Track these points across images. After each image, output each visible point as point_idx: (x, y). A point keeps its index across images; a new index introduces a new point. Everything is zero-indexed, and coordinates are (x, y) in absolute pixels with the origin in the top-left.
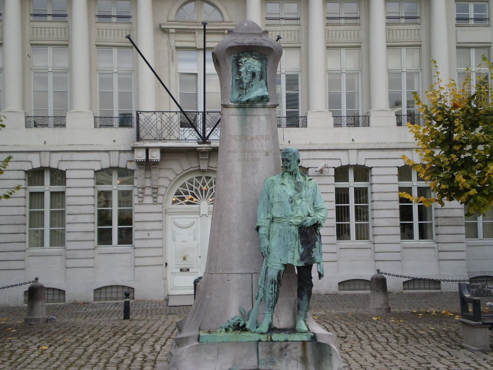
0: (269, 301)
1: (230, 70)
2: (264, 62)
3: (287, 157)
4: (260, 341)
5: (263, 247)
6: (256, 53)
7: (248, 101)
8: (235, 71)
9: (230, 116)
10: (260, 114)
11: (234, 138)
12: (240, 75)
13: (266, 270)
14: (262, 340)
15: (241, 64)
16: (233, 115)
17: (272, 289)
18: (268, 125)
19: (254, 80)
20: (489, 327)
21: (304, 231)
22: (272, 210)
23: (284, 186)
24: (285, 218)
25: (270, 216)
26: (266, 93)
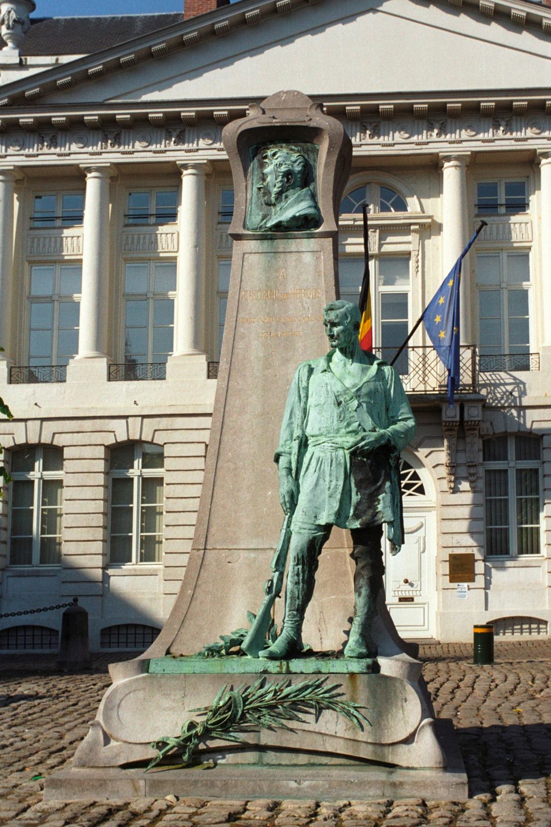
4: (265, 672)
12: (264, 180)
14: (269, 670)
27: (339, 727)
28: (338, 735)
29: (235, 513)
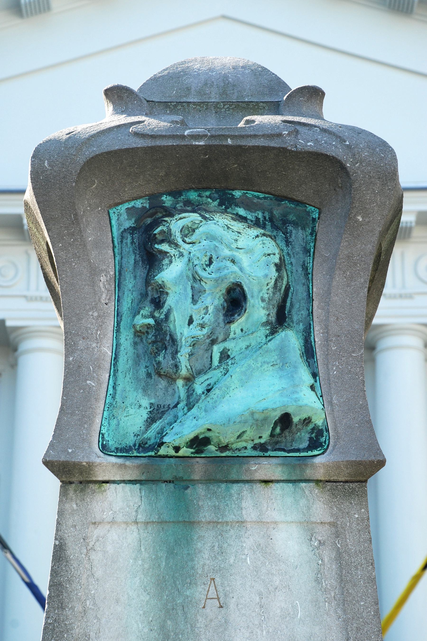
1: (104, 281)
2: (298, 235)
6: (250, 194)
7: (199, 443)
10: (276, 516)
12: (158, 304)
15: (165, 247)
18: (318, 581)
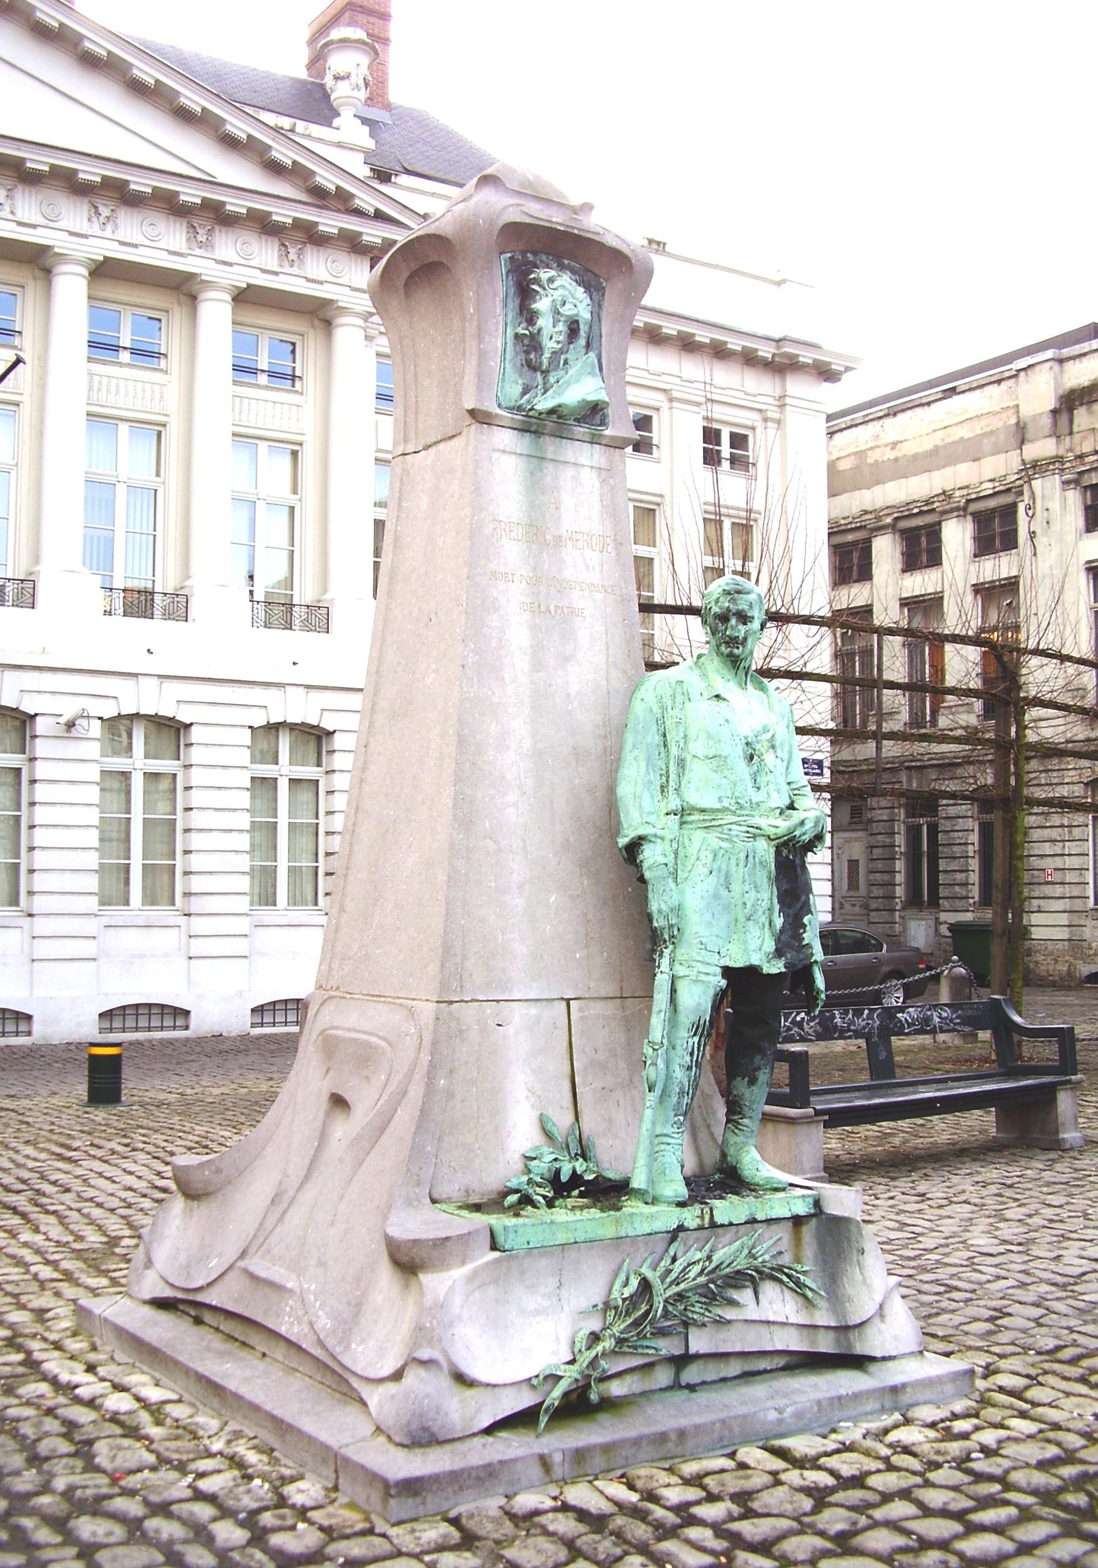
0: (682, 1093)
1: (499, 300)
3: (743, 606)
4: (681, 1228)
5: (664, 907)
6: (573, 264)
7: (552, 411)
8: (513, 304)
9: (496, 455)
11: (507, 529)
13: (673, 991)
14: (686, 1224)
16: (504, 451)
17: (692, 1054)
19: (572, 346)
20: (825, 1121)
21: (787, 857)
22: (683, 783)
23: (722, 704)
24: (734, 813)
25: (674, 803)
26: (603, 396)
27: (787, 1306)
28: (790, 1321)
29: (503, 934)
